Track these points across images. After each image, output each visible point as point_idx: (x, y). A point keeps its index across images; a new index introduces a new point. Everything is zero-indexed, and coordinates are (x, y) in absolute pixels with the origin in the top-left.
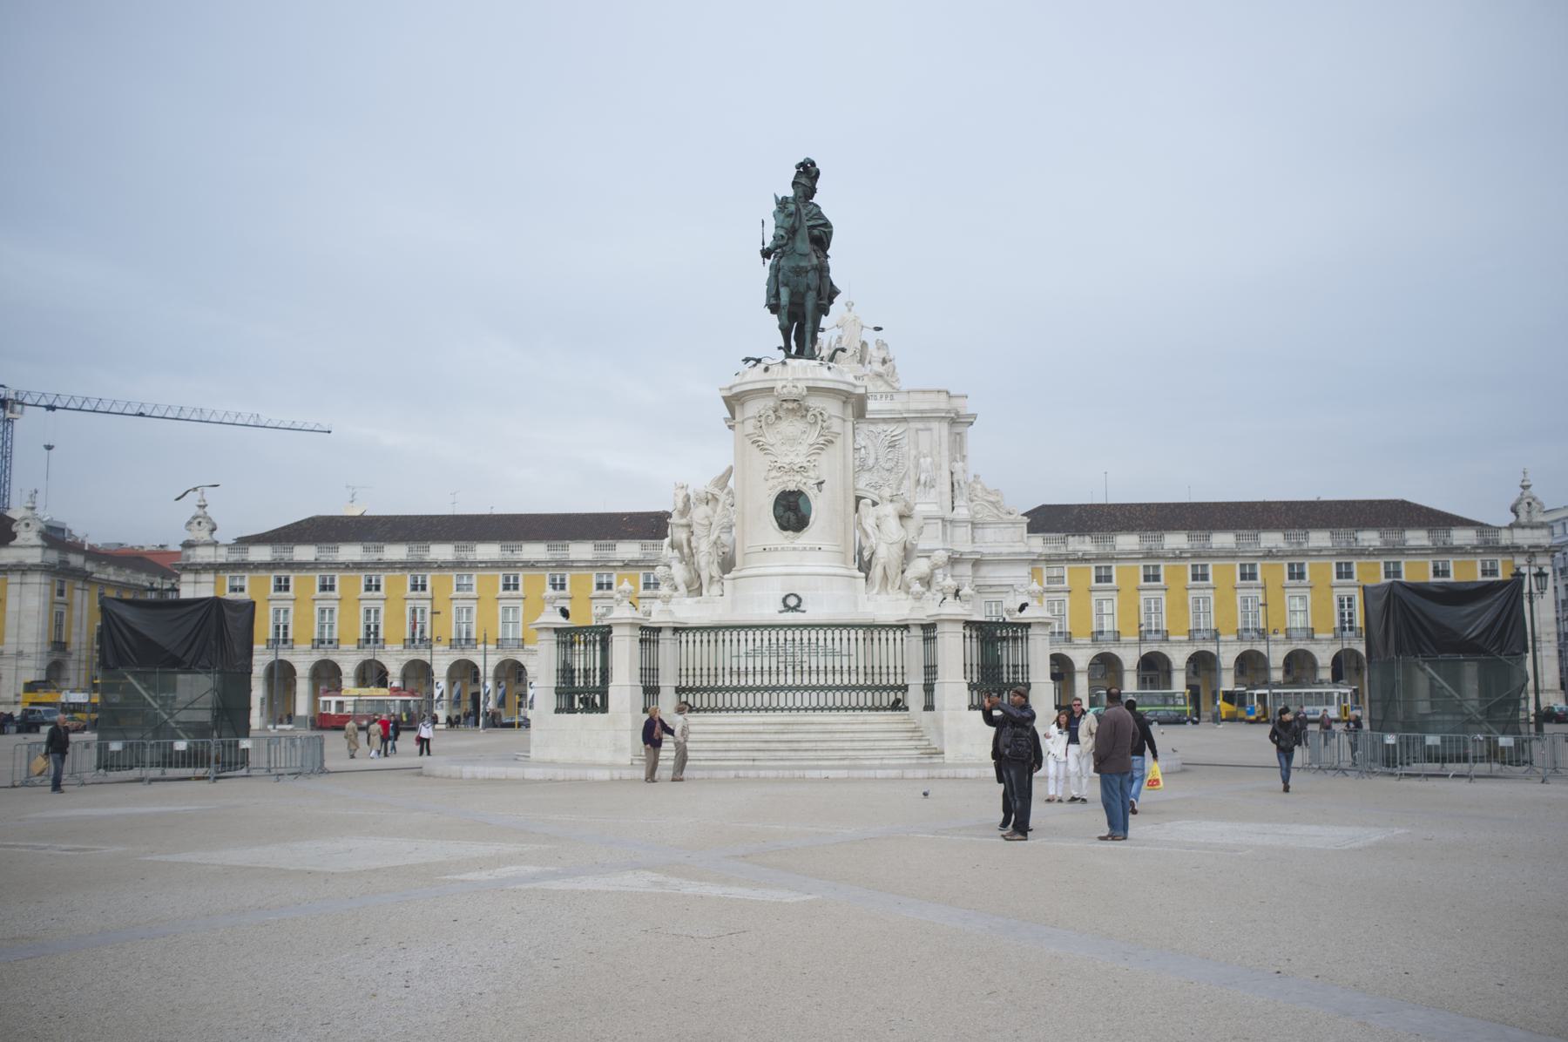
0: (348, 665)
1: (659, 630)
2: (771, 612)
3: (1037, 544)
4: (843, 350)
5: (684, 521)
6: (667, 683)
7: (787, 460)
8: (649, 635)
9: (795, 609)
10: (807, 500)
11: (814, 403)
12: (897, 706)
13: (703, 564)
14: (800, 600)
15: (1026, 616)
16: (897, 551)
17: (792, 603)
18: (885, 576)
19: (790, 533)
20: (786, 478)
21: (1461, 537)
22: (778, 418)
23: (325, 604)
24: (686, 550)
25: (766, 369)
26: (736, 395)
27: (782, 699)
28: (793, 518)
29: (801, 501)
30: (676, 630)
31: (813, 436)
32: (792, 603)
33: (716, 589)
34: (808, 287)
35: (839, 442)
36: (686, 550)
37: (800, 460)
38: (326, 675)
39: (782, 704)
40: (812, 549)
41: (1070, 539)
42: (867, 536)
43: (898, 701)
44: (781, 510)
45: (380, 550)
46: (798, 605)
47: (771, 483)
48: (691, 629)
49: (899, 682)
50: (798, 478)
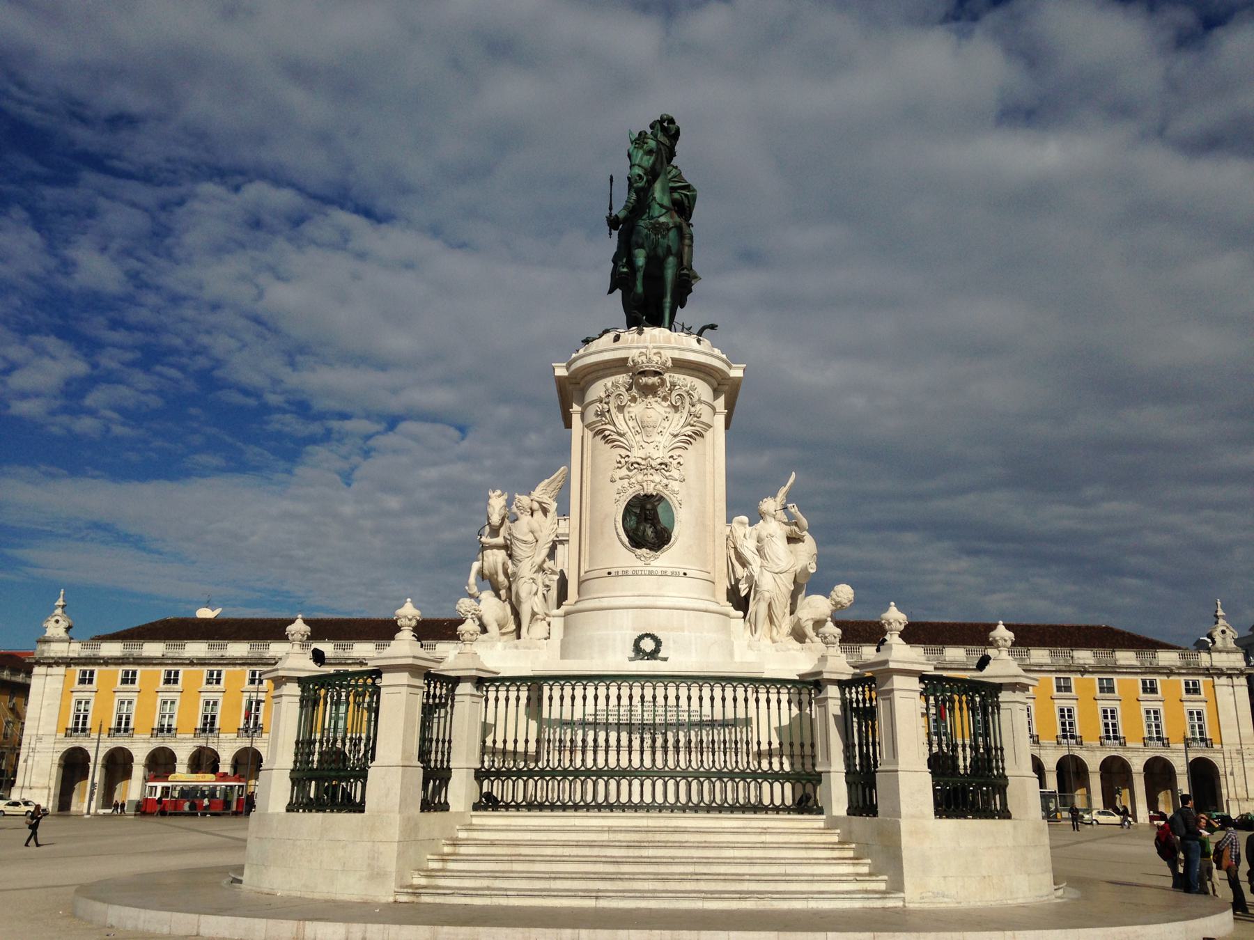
0: (183, 751)
1: (457, 680)
2: (619, 660)
4: (713, 327)
5: (499, 540)
6: (463, 761)
7: (642, 453)
8: (439, 691)
9: (653, 655)
10: (669, 509)
12: (805, 804)
13: (523, 594)
14: (658, 643)
17: (647, 646)
20: (640, 477)
21: (1166, 658)
22: (634, 400)
23: (167, 696)
24: (501, 578)
27: (634, 791)
28: (649, 531)
29: (660, 510)
30: (480, 682)
31: (677, 422)
32: (647, 646)
33: (539, 629)
35: (708, 435)
36: (501, 578)
38: (161, 763)
42: (744, 563)
44: (632, 522)
45: (224, 647)
47: (619, 484)
48: (503, 680)
50: (657, 478)
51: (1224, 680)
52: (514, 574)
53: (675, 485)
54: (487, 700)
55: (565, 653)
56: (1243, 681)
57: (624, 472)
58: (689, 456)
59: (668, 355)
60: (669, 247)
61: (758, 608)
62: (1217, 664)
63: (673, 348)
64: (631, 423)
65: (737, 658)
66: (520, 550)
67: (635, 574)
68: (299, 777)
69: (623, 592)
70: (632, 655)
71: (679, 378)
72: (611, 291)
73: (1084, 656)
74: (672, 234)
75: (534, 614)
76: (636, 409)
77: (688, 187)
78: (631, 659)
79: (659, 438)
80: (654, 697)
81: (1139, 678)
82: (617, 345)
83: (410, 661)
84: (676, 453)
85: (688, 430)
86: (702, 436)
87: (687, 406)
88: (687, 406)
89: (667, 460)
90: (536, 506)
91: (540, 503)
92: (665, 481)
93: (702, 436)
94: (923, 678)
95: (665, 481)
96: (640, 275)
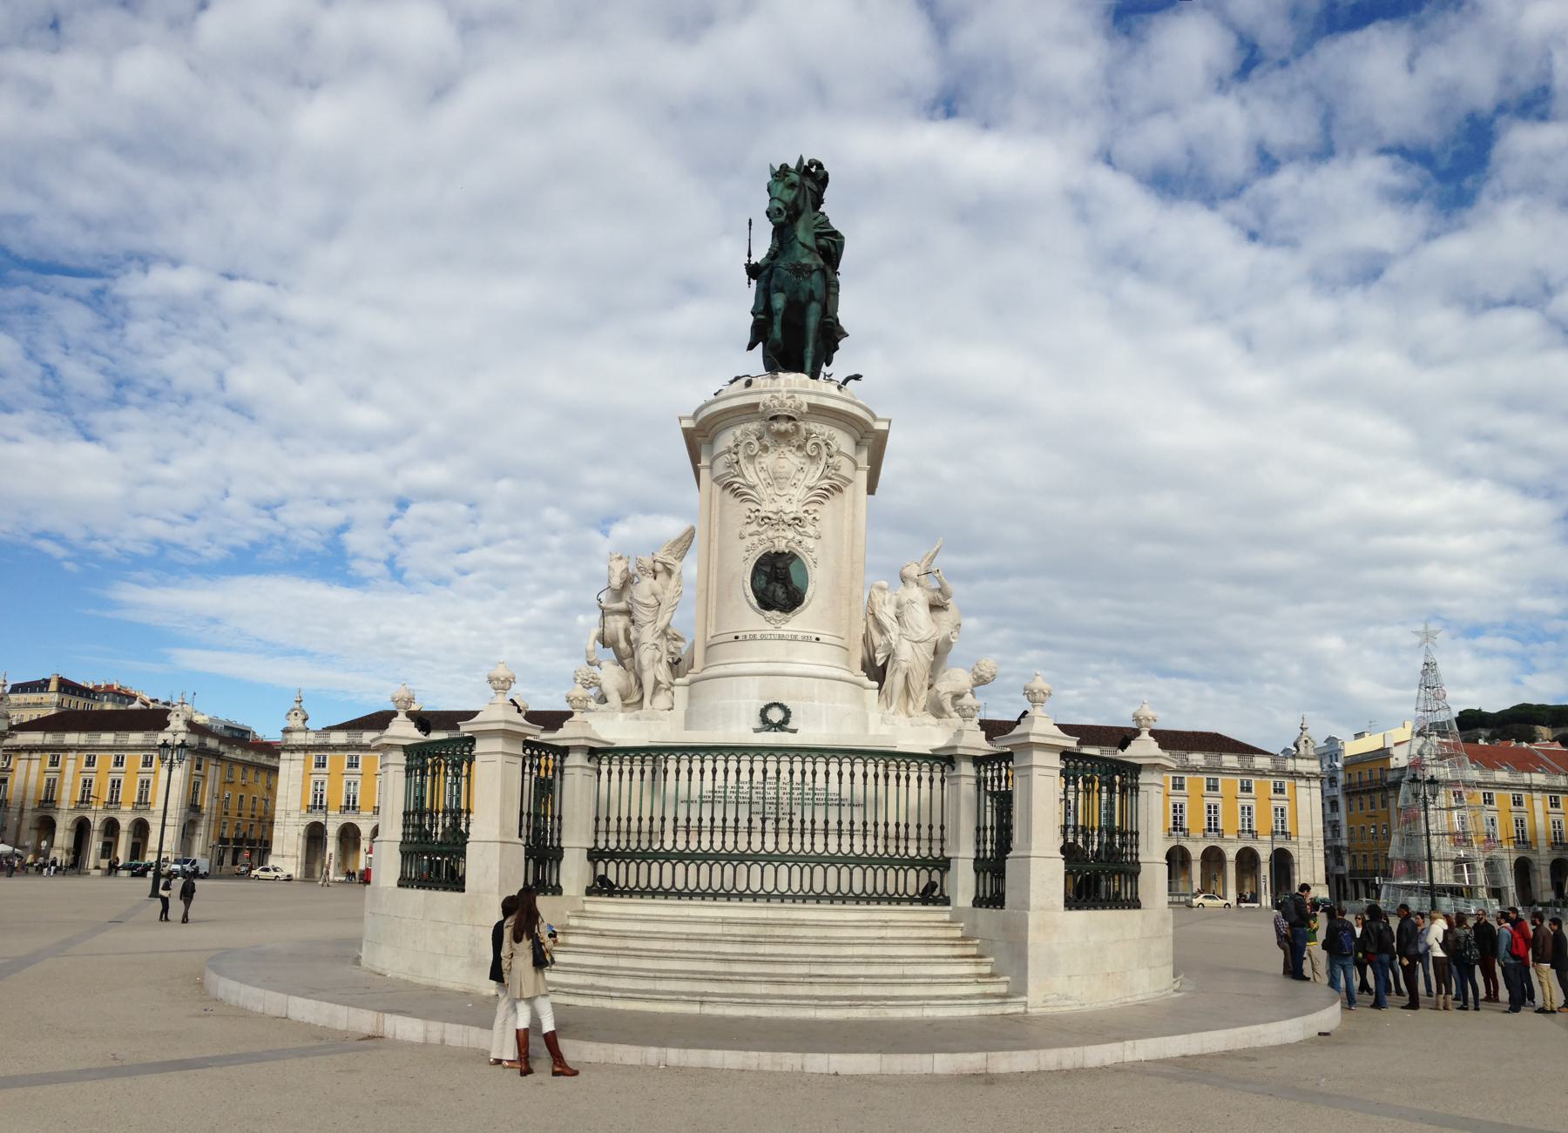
2: (743, 731)
4: (857, 377)
5: (622, 605)
6: (575, 839)
7: (774, 508)
9: (781, 726)
11: (821, 429)
17: (775, 716)
19: (774, 613)
20: (771, 534)
22: (765, 449)
24: (623, 645)
25: (749, 384)
27: (755, 877)
28: (780, 592)
29: (793, 569)
31: (813, 475)
32: (775, 716)
33: (662, 700)
34: (811, 297)
35: (848, 490)
36: (623, 645)
37: (793, 509)
39: (755, 887)
40: (806, 639)
42: (882, 630)
44: (762, 582)
46: (786, 721)
47: (748, 541)
49: (936, 853)
50: (790, 534)
52: (637, 640)
53: (809, 543)
54: (599, 773)
55: (689, 723)
58: (827, 510)
59: (805, 400)
60: (811, 292)
63: (810, 393)
64: (762, 475)
65: (872, 732)
66: (642, 615)
67: (763, 638)
68: (408, 852)
69: (751, 658)
70: (759, 725)
71: (816, 427)
72: (751, 347)
74: (816, 277)
75: (657, 683)
76: (768, 460)
77: (835, 233)
78: (756, 731)
79: (793, 491)
80: (778, 772)
82: (750, 389)
83: (502, 726)
84: (811, 507)
85: (825, 483)
86: (841, 491)
87: (824, 456)
88: (824, 456)
89: (801, 515)
90: (659, 567)
91: (664, 564)
92: (799, 538)
93: (841, 491)
95: (799, 538)
96: (778, 320)
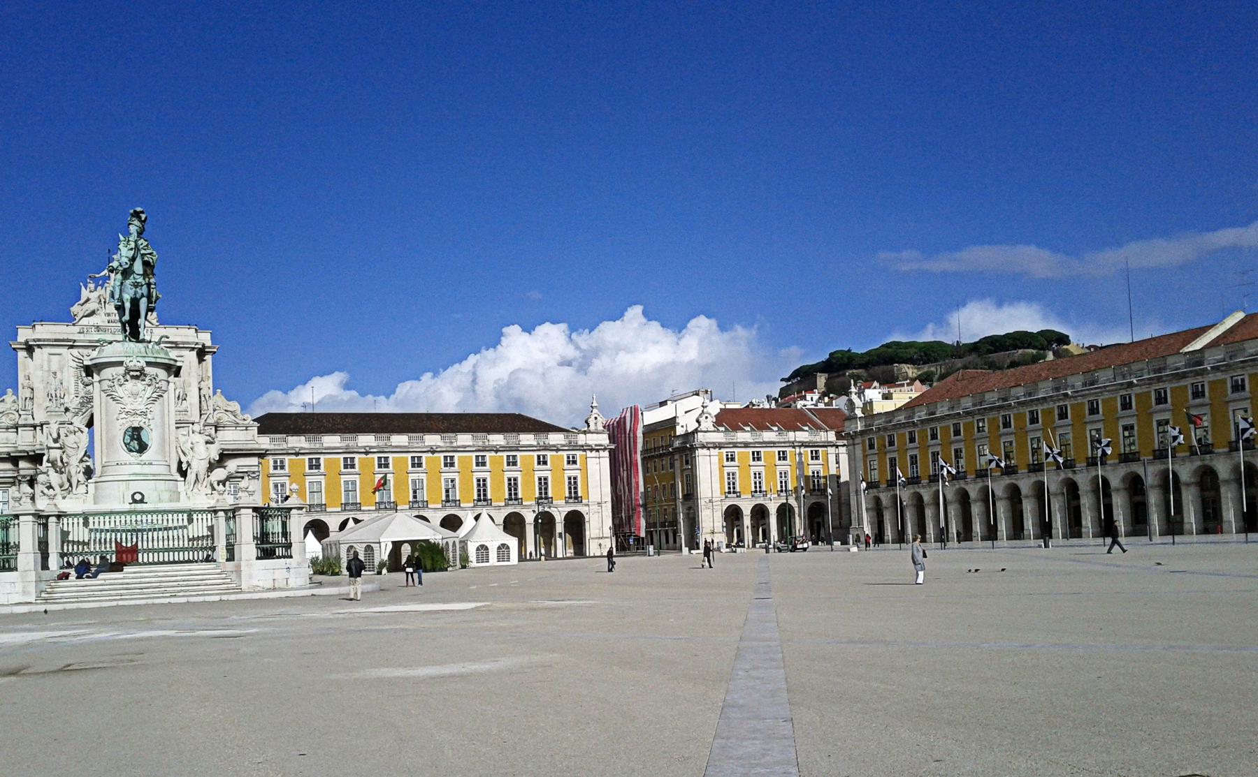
1: (48, 516)
3: (265, 442)
5: (57, 445)
8: (42, 519)
9: (142, 501)
12: (208, 560)
13: (73, 473)
15: (288, 504)
16: (205, 465)
18: (197, 480)
21: (555, 439)
26: (95, 365)
33: (82, 489)
35: (165, 395)
37: (142, 408)
41: (290, 438)
43: (208, 556)
47: (121, 421)
48: (70, 515)
50: (140, 418)
51: (594, 454)
56: (606, 454)
57: (123, 415)
61: (191, 476)
62: (589, 442)
66: (68, 450)
73: (497, 439)
81: (535, 454)
94: (255, 509)
